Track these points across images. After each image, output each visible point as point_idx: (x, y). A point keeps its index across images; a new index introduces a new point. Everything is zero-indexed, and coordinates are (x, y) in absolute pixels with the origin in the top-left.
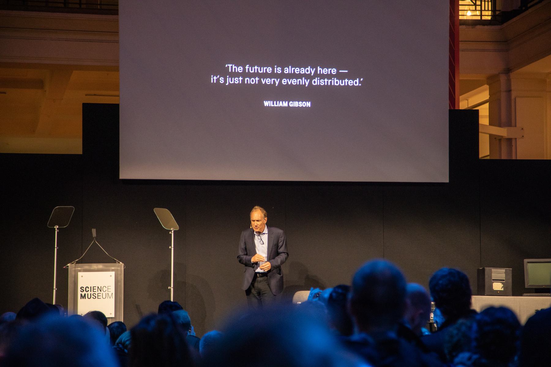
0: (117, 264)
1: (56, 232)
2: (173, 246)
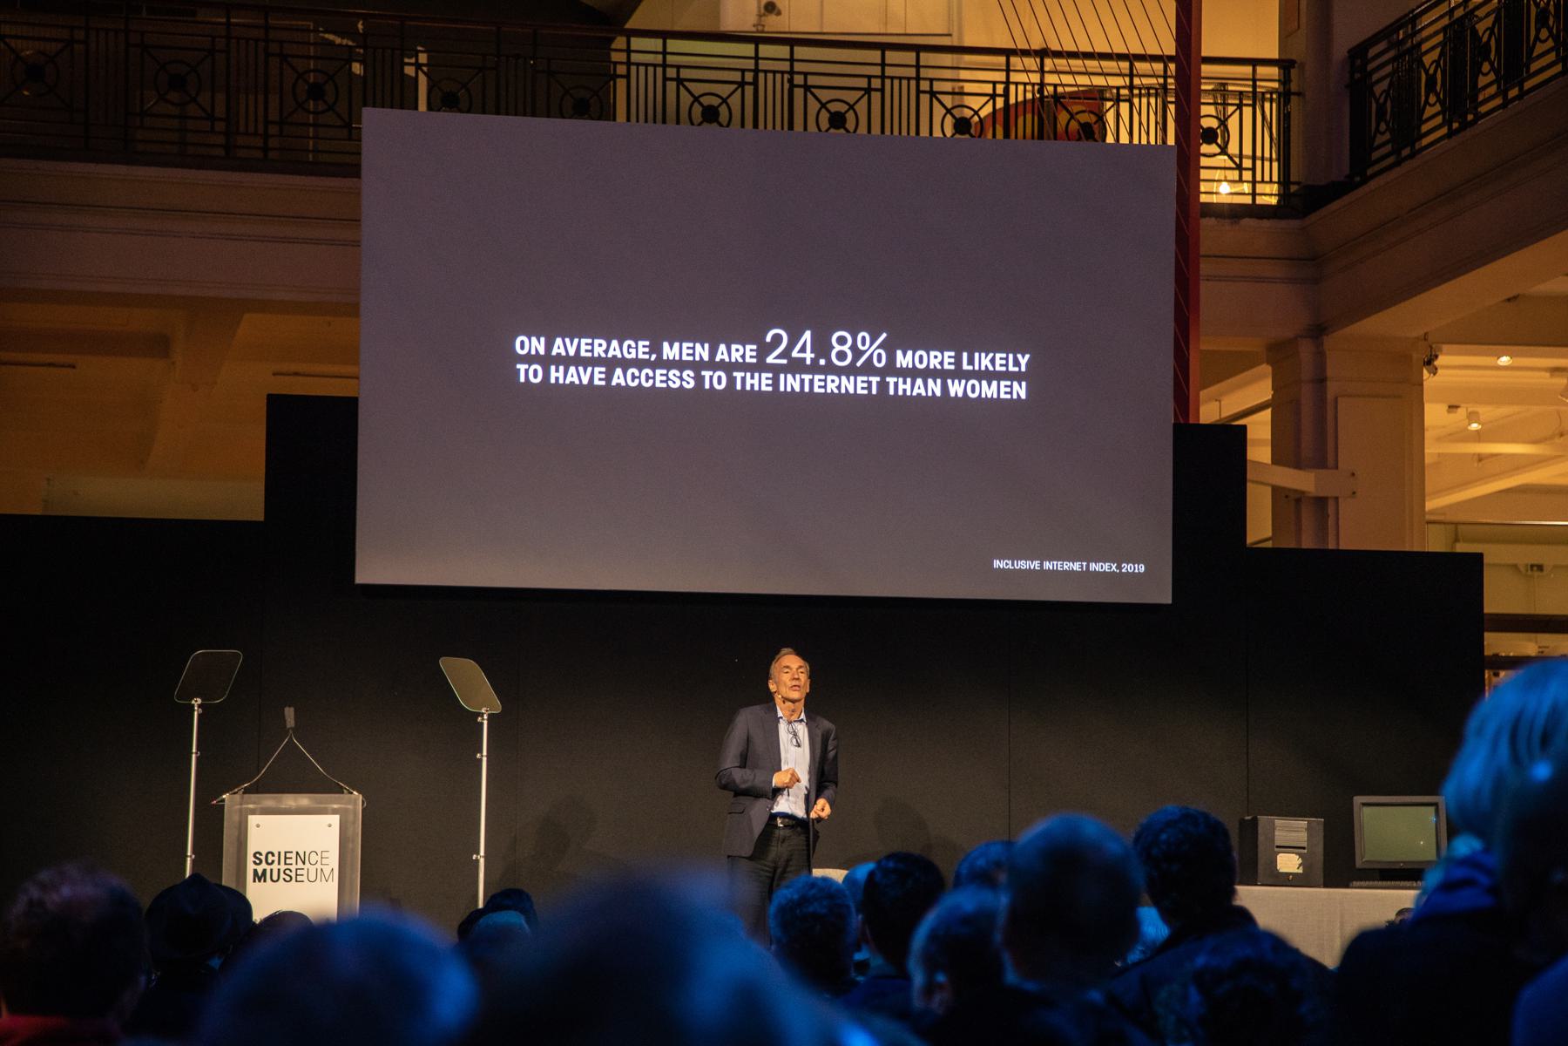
0: (346, 796)
1: (196, 713)
2: (485, 753)
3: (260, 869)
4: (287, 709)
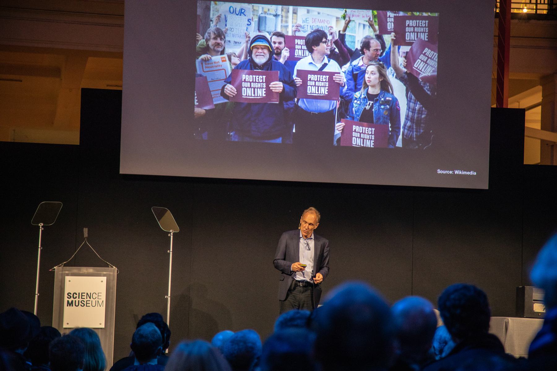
0: (110, 268)
1: (41, 230)
2: (171, 250)
3: (70, 300)
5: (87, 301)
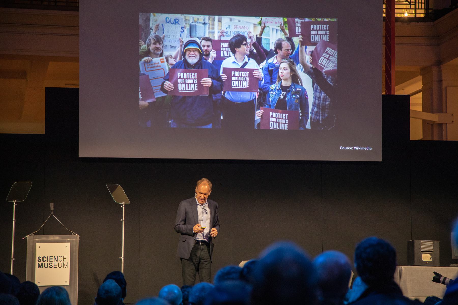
0: (73, 236)
1: (14, 205)
2: (123, 219)
3: (40, 263)
4: (51, 204)
5: (54, 263)
